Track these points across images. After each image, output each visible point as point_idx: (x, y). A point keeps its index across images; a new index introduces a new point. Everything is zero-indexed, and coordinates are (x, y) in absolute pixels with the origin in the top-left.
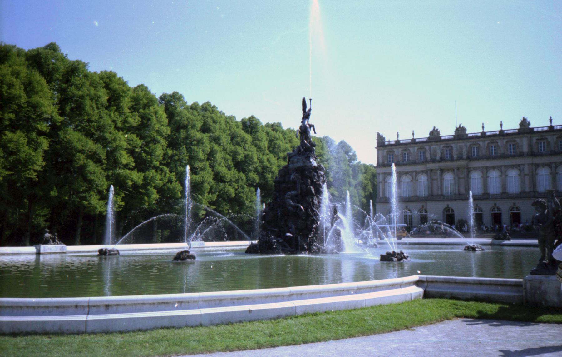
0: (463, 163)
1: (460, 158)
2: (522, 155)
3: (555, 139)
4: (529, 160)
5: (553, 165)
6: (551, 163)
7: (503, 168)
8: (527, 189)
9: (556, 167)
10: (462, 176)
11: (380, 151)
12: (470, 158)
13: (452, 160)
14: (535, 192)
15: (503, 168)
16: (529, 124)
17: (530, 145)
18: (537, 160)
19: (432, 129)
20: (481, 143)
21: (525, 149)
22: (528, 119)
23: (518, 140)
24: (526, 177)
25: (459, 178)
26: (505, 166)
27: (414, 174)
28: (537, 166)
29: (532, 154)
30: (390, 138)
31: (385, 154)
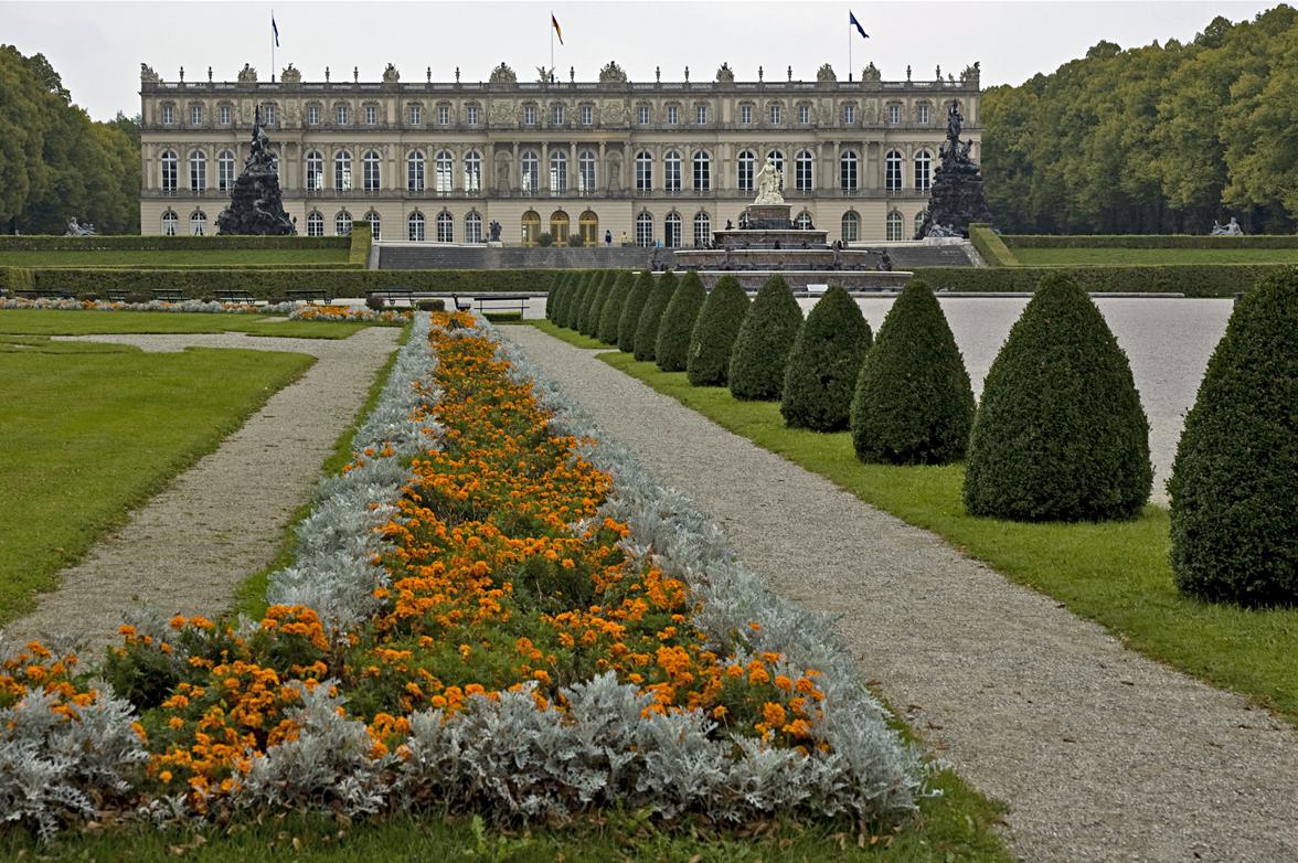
0: (297, 137)
1: (291, 129)
2: (384, 129)
3: (434, 106)
4: (396, 139)
5: (430, 148)
6: (427, 144)
7: (357, 147)
8: (392, 186)
9: (434, 151)
10: (293, 158)
11: (148, 101)
12: (306, 129)
13: (279, 130)
14: (402, 189)
15: (357, 147)
16: (398, 76)
17: (398, 111)
18: (408, 139)
19: (242, 68)
20: (323, 101)
21: (391, 119)
22: (397, 68)
23: (380, 102)
24: (392, 164)
25: (288, 161)
26: (361, 145)
27: (212, 148)
28: (406, 146)
29: (401, 129)
30: (169, 77)
31: (158, 106)
